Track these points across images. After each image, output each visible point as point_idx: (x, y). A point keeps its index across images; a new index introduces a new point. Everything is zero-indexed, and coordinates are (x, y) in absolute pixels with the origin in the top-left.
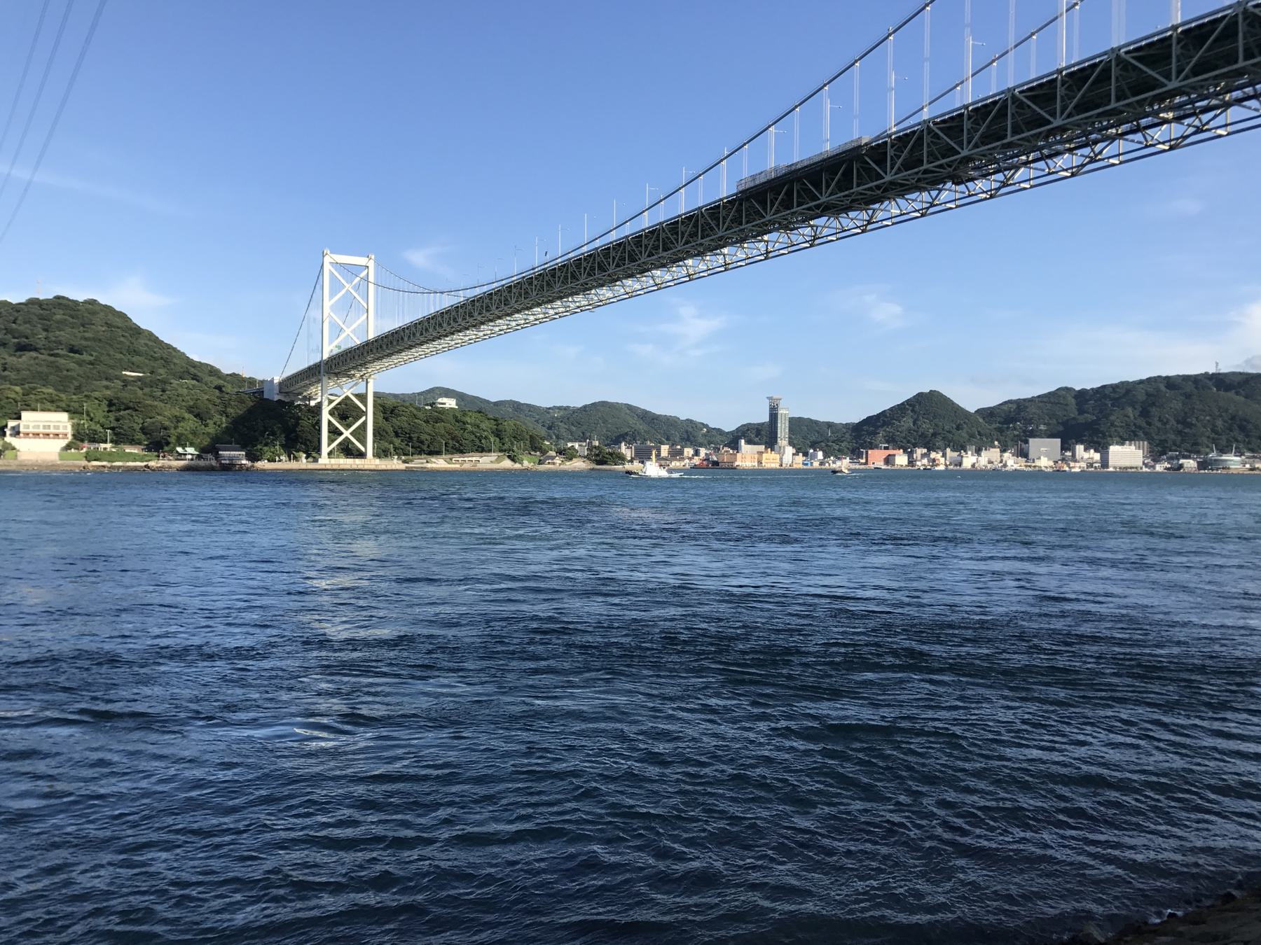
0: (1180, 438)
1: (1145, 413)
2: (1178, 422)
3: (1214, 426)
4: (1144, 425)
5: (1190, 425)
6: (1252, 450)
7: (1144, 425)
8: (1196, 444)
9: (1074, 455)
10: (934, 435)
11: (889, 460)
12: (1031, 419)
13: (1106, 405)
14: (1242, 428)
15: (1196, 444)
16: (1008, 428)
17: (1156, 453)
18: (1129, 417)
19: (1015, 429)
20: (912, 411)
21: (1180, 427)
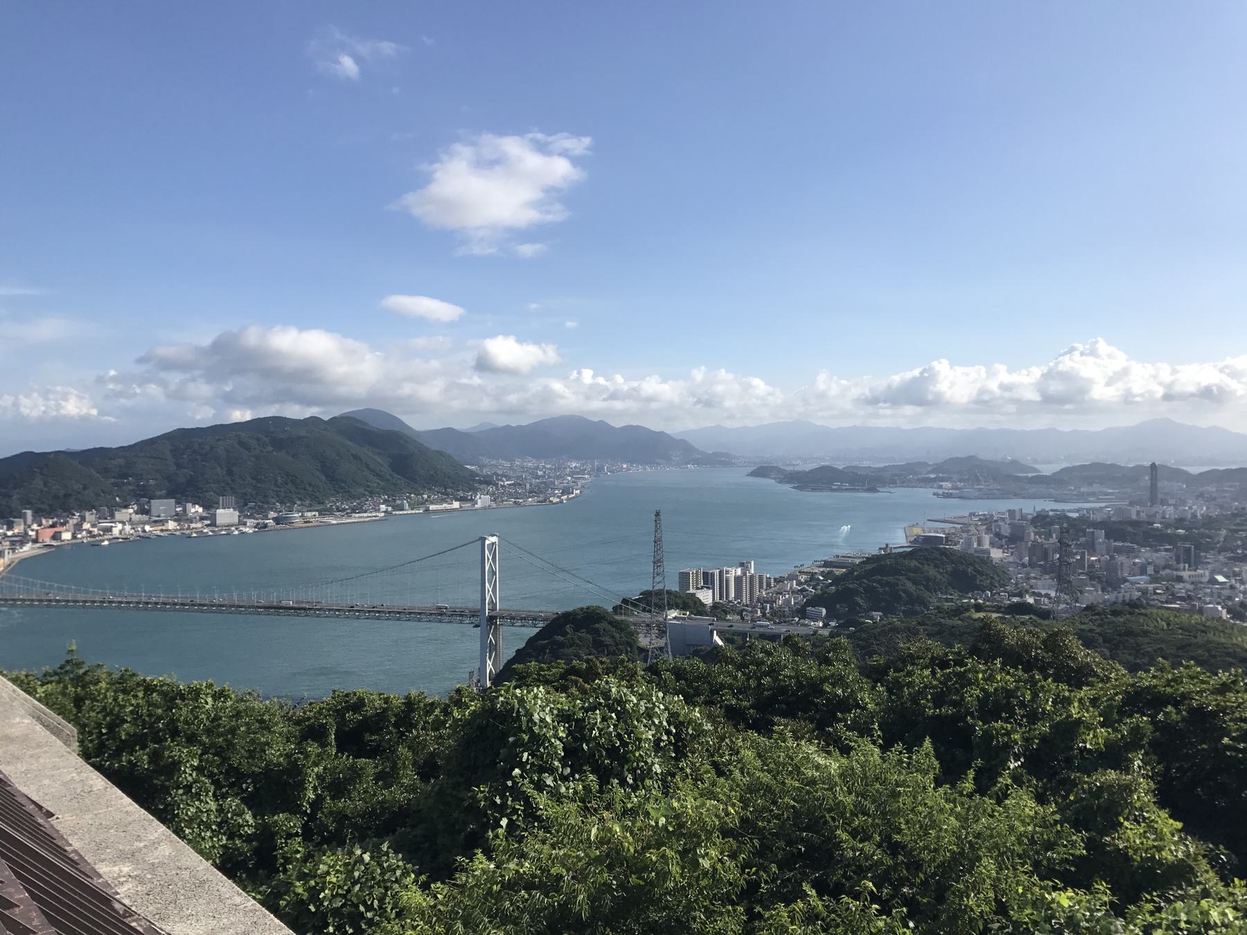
0: (254, 492)
1: (230, 473)
2: (252, 478)
3: (276, 481)
4: (230, 482)
5: (258, 481)
6: (300, 499)
7: (230, 482)
8: (267, 496)
9: (185, 510)
10: (67, 496)
11: (56, 536)
12: (142, 475)
13: (197, 460)
14: (293, 482)
15: (267, 496)
16: (124, 484)
17: (241, 506)
18: (219, 476)
19: (129, 483)
20: (42, 474)
21: (254, 482)
